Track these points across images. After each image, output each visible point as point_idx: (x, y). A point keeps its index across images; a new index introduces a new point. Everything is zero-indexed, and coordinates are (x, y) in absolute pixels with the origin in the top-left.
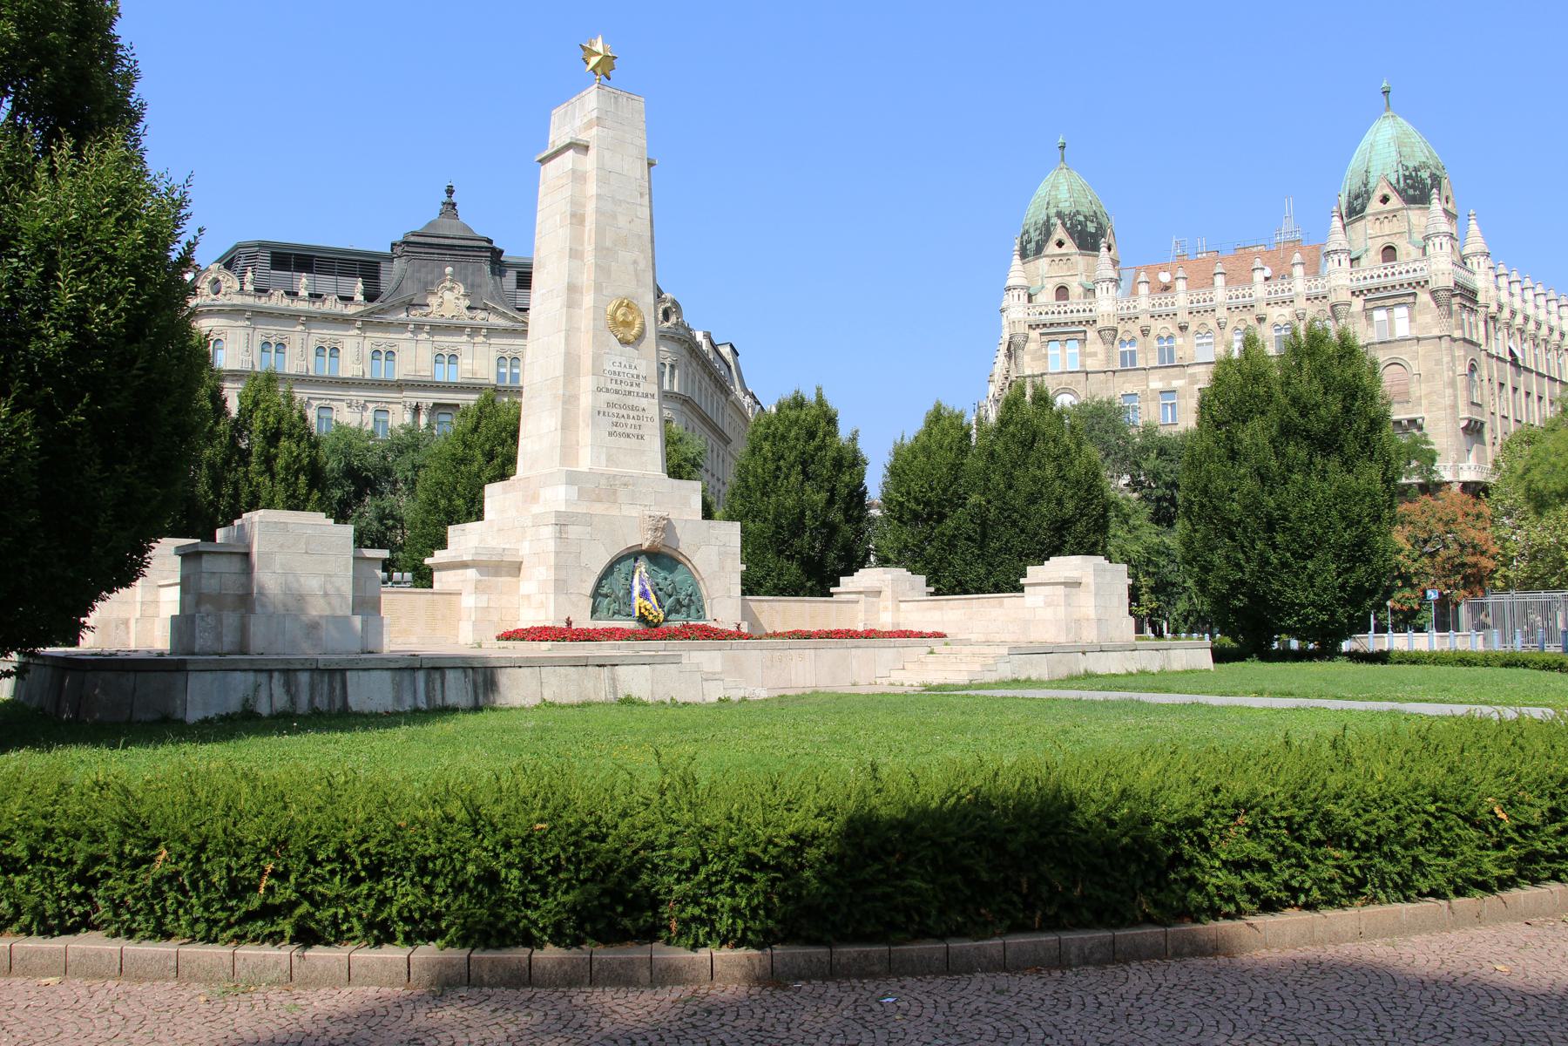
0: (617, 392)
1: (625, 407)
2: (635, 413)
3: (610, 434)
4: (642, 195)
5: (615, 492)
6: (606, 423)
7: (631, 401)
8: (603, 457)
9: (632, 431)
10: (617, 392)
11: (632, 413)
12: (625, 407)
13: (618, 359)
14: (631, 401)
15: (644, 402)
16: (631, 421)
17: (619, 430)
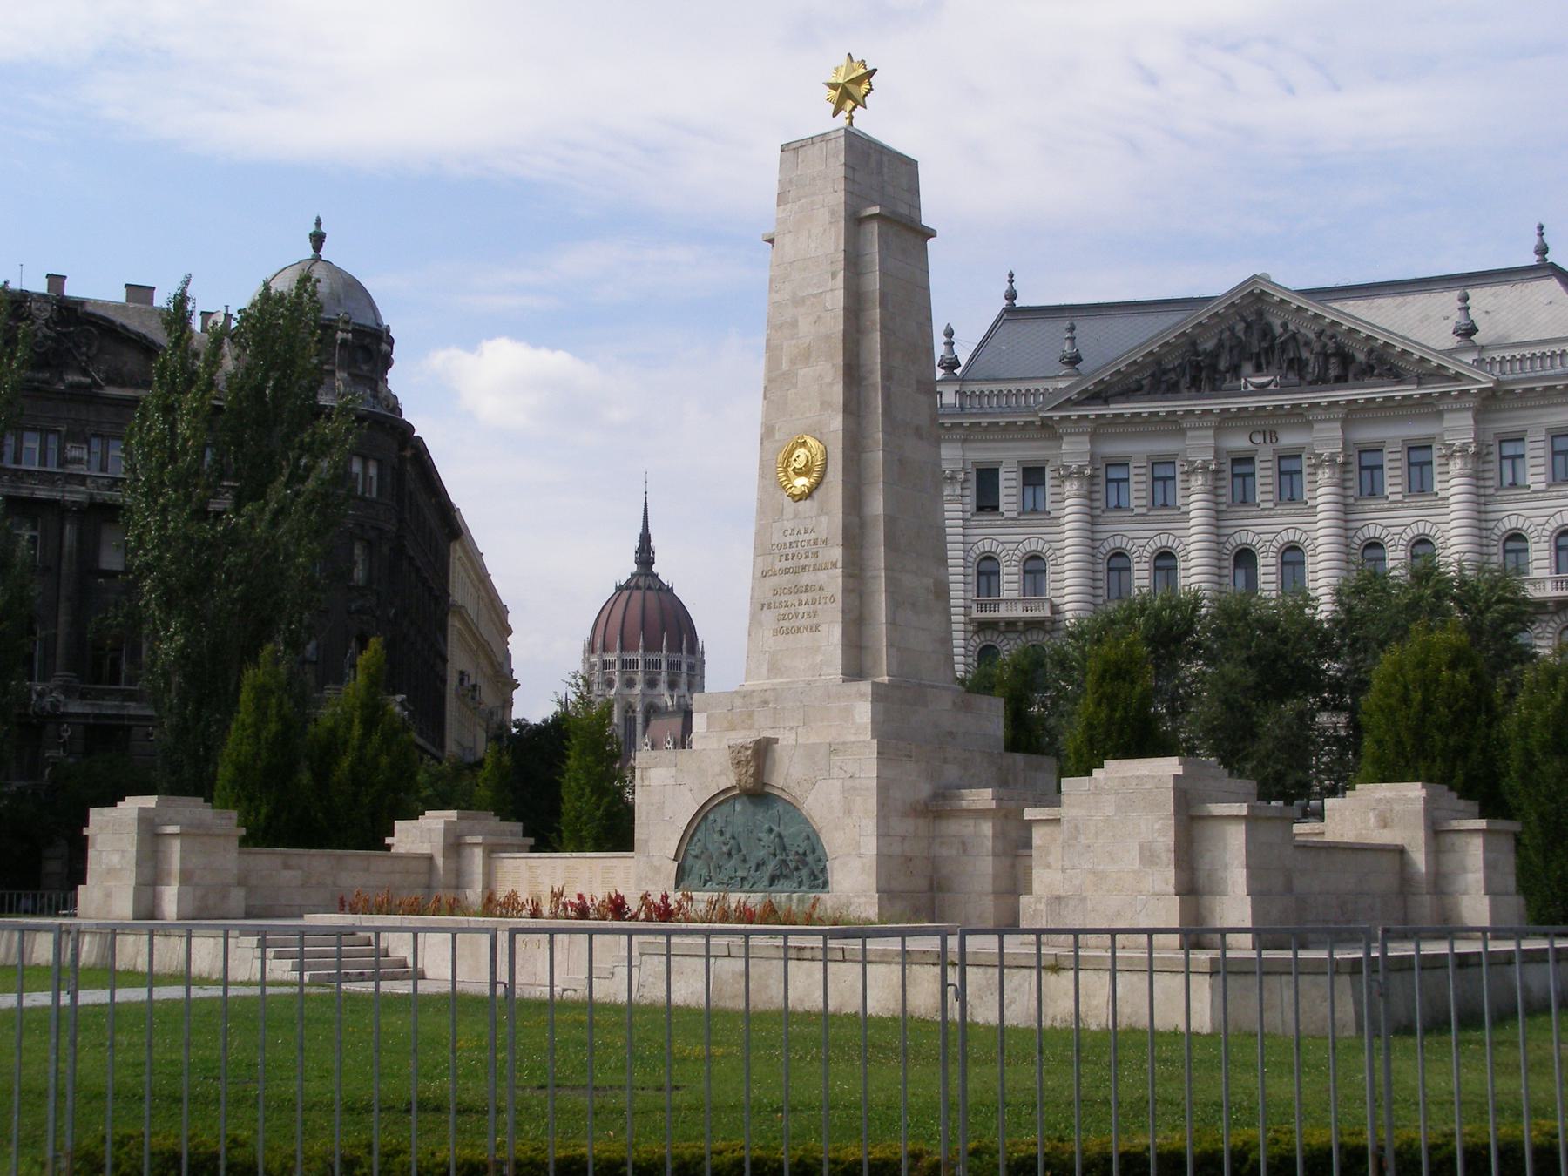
0: (786, 571)
1: (796, 590)
2: (809, 596)
3: (775, 633)
4: (834, 275)
5: (750, 715)
6: (769, 617)
7: (806, 579)
8: (765, 670)
9: (806, 622)
10: (786, 571)
11: (804, 597)
12: (796, 590)
13: (789, 525)
14: (806, 579)
15: (822, 576)
16: (804, 609)
17: (785, 624)
